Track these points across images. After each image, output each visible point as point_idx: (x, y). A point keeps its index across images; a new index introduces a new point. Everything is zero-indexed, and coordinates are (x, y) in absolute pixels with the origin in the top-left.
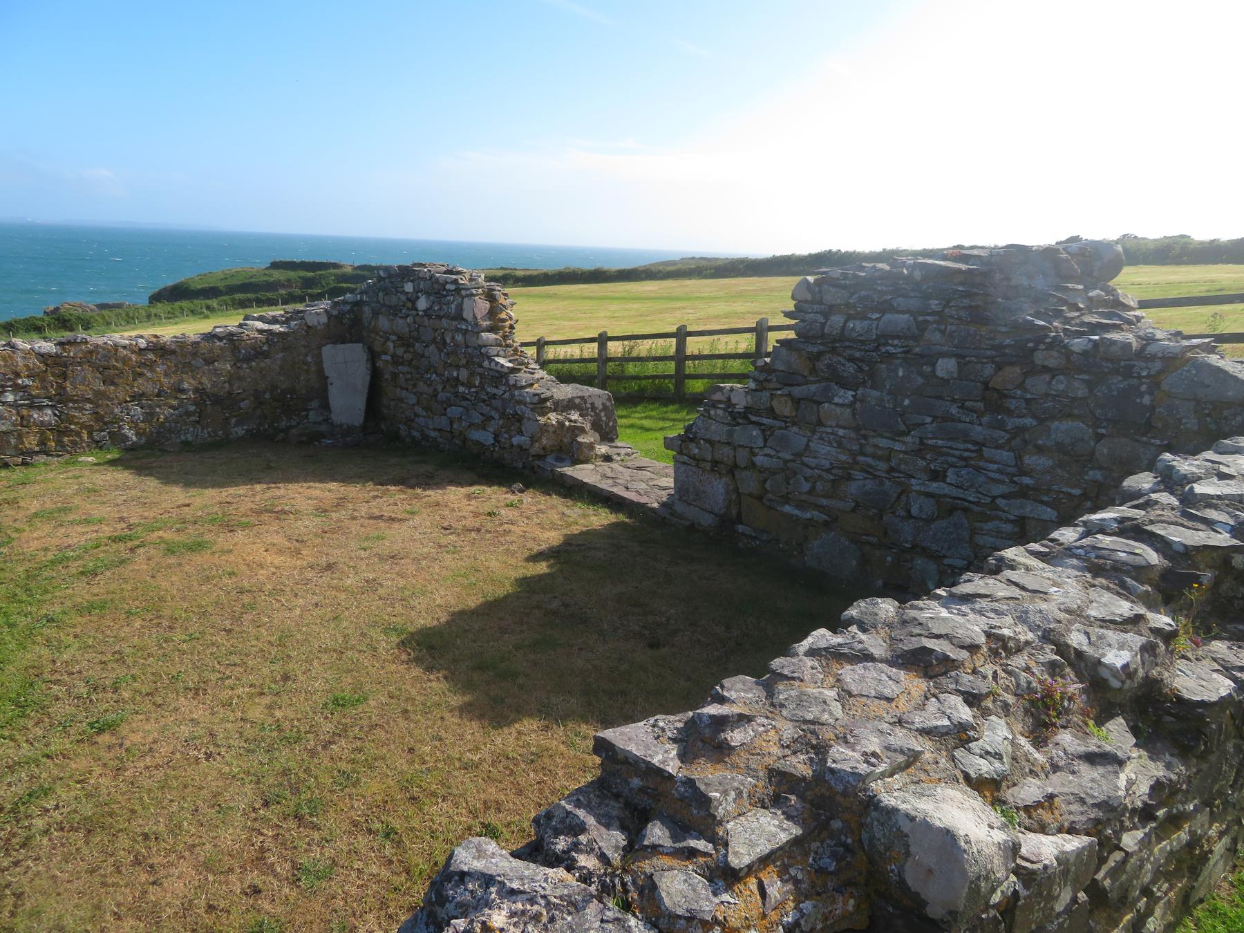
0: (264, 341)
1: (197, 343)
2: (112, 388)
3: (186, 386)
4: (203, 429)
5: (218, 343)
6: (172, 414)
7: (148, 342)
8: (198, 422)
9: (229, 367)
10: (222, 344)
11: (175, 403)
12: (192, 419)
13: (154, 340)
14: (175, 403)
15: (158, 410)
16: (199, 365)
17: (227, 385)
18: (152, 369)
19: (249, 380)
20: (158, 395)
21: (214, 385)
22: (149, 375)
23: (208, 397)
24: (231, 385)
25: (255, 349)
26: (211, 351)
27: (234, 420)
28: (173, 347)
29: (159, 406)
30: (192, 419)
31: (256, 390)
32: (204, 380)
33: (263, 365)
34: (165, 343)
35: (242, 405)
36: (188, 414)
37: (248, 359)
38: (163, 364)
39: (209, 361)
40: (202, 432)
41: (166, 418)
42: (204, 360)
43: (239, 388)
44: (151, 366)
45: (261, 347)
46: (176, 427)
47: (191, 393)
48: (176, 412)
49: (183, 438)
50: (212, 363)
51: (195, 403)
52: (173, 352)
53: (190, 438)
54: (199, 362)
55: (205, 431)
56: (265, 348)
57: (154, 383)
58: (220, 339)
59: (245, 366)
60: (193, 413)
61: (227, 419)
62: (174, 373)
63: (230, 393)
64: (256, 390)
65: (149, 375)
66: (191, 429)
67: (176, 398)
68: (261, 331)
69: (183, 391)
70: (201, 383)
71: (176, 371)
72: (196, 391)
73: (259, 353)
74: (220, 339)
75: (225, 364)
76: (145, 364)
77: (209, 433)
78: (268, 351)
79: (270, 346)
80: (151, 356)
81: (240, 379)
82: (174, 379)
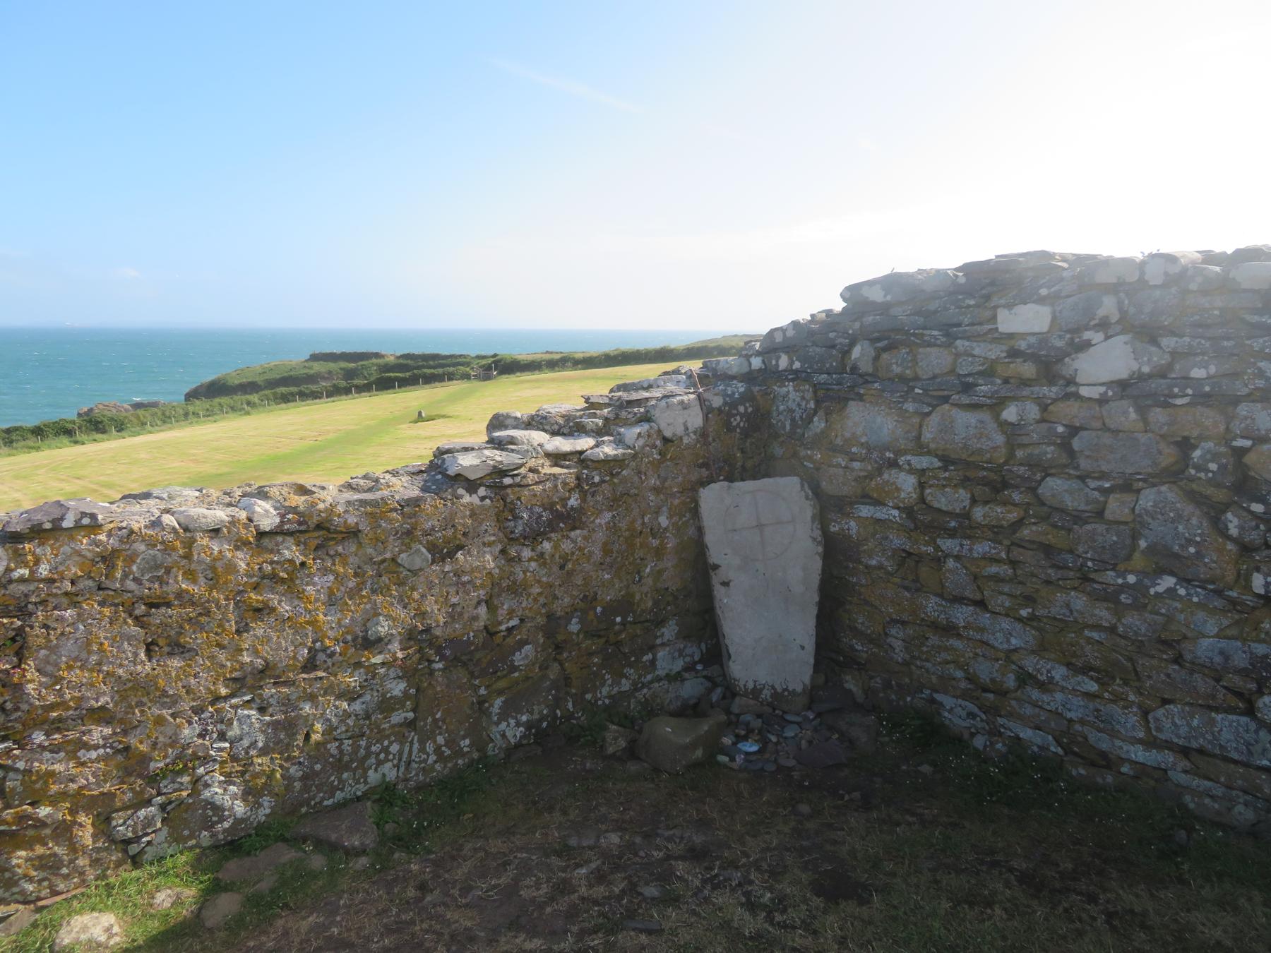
0: (572, 482)
1: (415, 502)
2: (176, 663)
3: (383, 628)
4: (422, 742)
5: (467, 499)
6: (347, 715)
7: (284, 511)
8: (411, 724)
9: (489, 562)
10: (475, 499)
11: (352, 680)
12: (397, 717)
13: (299, 501)
14: (352, 680)
15: (307, 708)
16: (418, 563)
17: (483, 610)
18: (294, 592)
19: (536, 590)
20: (310, 665)
21: (454, 615)
22: (285, 608)
23: (439, 651)
24: (492, 608)
25: (550, 507)
26: (449, 522)
27: (498, 702)
28: (352, 520)
29: (312, 698)
30: (397, 717)
31: (550, 616)
32: (431, 606)
33: (567, 546)
34: (331, 510)
35: (518, 659)
36: (387, 705)
37: (533, 536)
38: (324, 571)
39: (442, 553)
40: (422, 750)
41: (330, 730)
42: (432, 548)
43: (511, 613)
44: (288, 581)
45: (564, 500)
46: (356, 748)
47: (395, 646)
48: (357, 706)
49: (373, 777)
50: (451, 555)
51: (408, 673)
52: (353, 533)
53: (391, 775)
54: (419, 556)
55: (430, 747)
56: (573, 502)
57: (298, 629)
58: (472, 486)
59: (527, 553)
60: (397, 703)
61: (481, 706)
62: (352, 594)
63: (490, 632)
64: (550, 616)
65: (285, 608)
66: (395, 748)
67: (358, 665)
68: (557, 458)
69: (370, 643)
70: (422, 615)
71: (359, 588)
72: (410, 636)
73: (559, 516)
74: (472, 486)
75: (481, 554)
76: (273, 577)
77: (438, 750)
78: (580, 510)
79: (584, 494)
80: (290, 551)
81: (516, 589)
82: (352, 614)
